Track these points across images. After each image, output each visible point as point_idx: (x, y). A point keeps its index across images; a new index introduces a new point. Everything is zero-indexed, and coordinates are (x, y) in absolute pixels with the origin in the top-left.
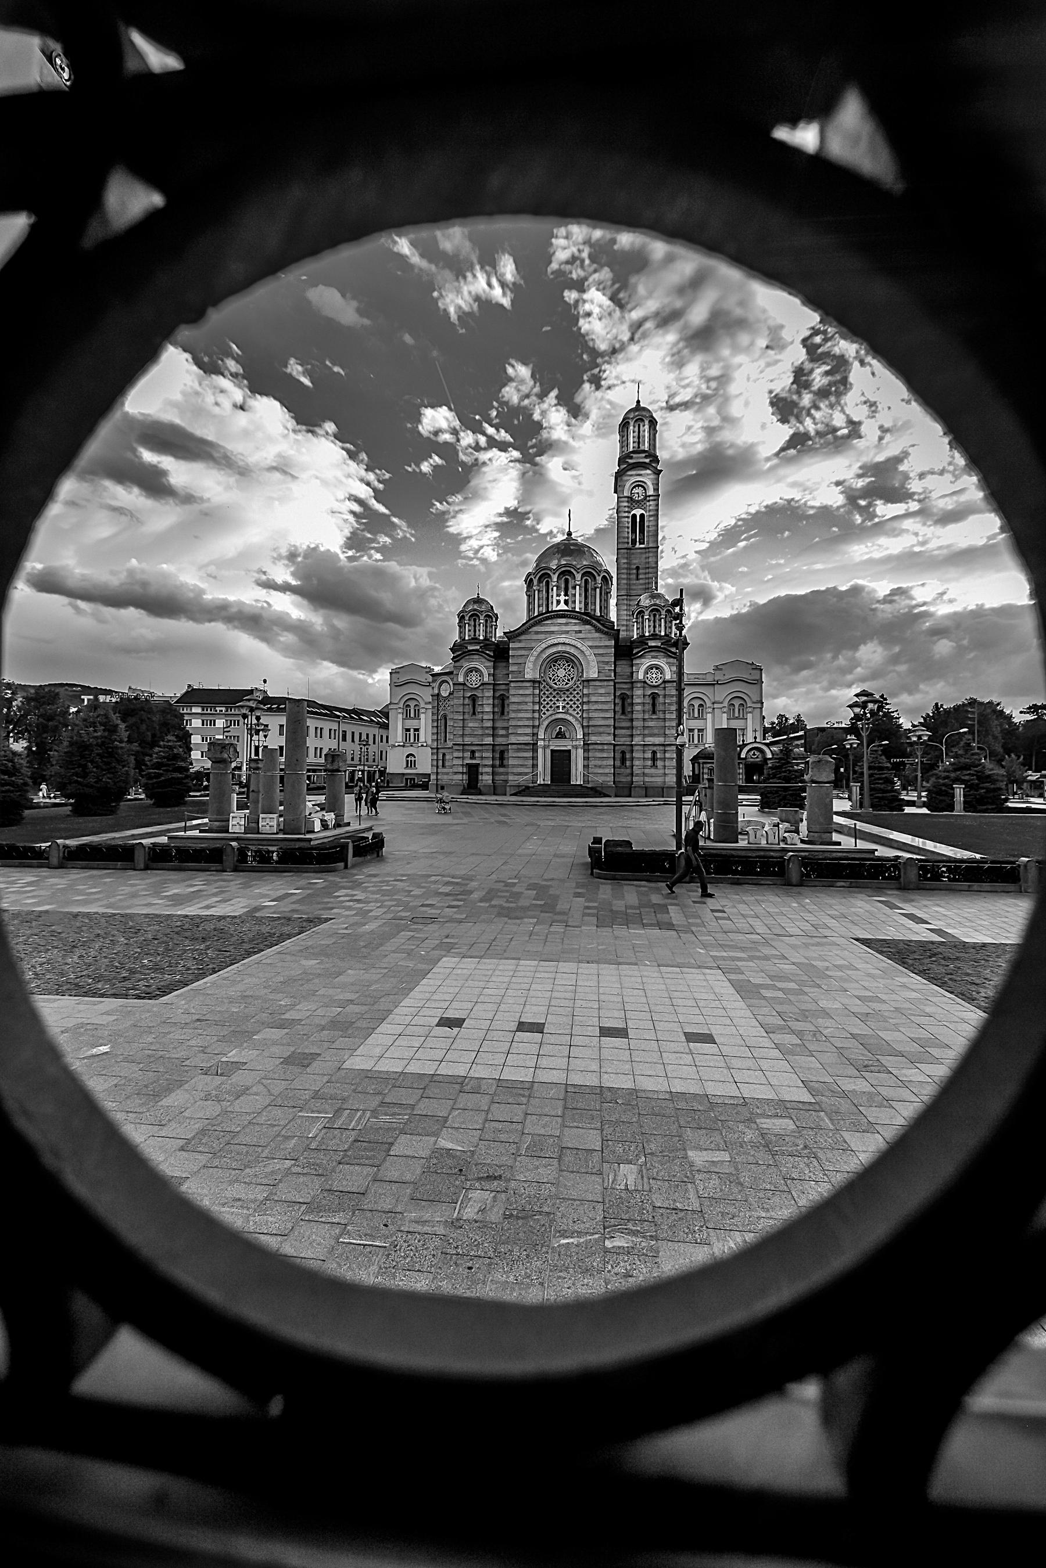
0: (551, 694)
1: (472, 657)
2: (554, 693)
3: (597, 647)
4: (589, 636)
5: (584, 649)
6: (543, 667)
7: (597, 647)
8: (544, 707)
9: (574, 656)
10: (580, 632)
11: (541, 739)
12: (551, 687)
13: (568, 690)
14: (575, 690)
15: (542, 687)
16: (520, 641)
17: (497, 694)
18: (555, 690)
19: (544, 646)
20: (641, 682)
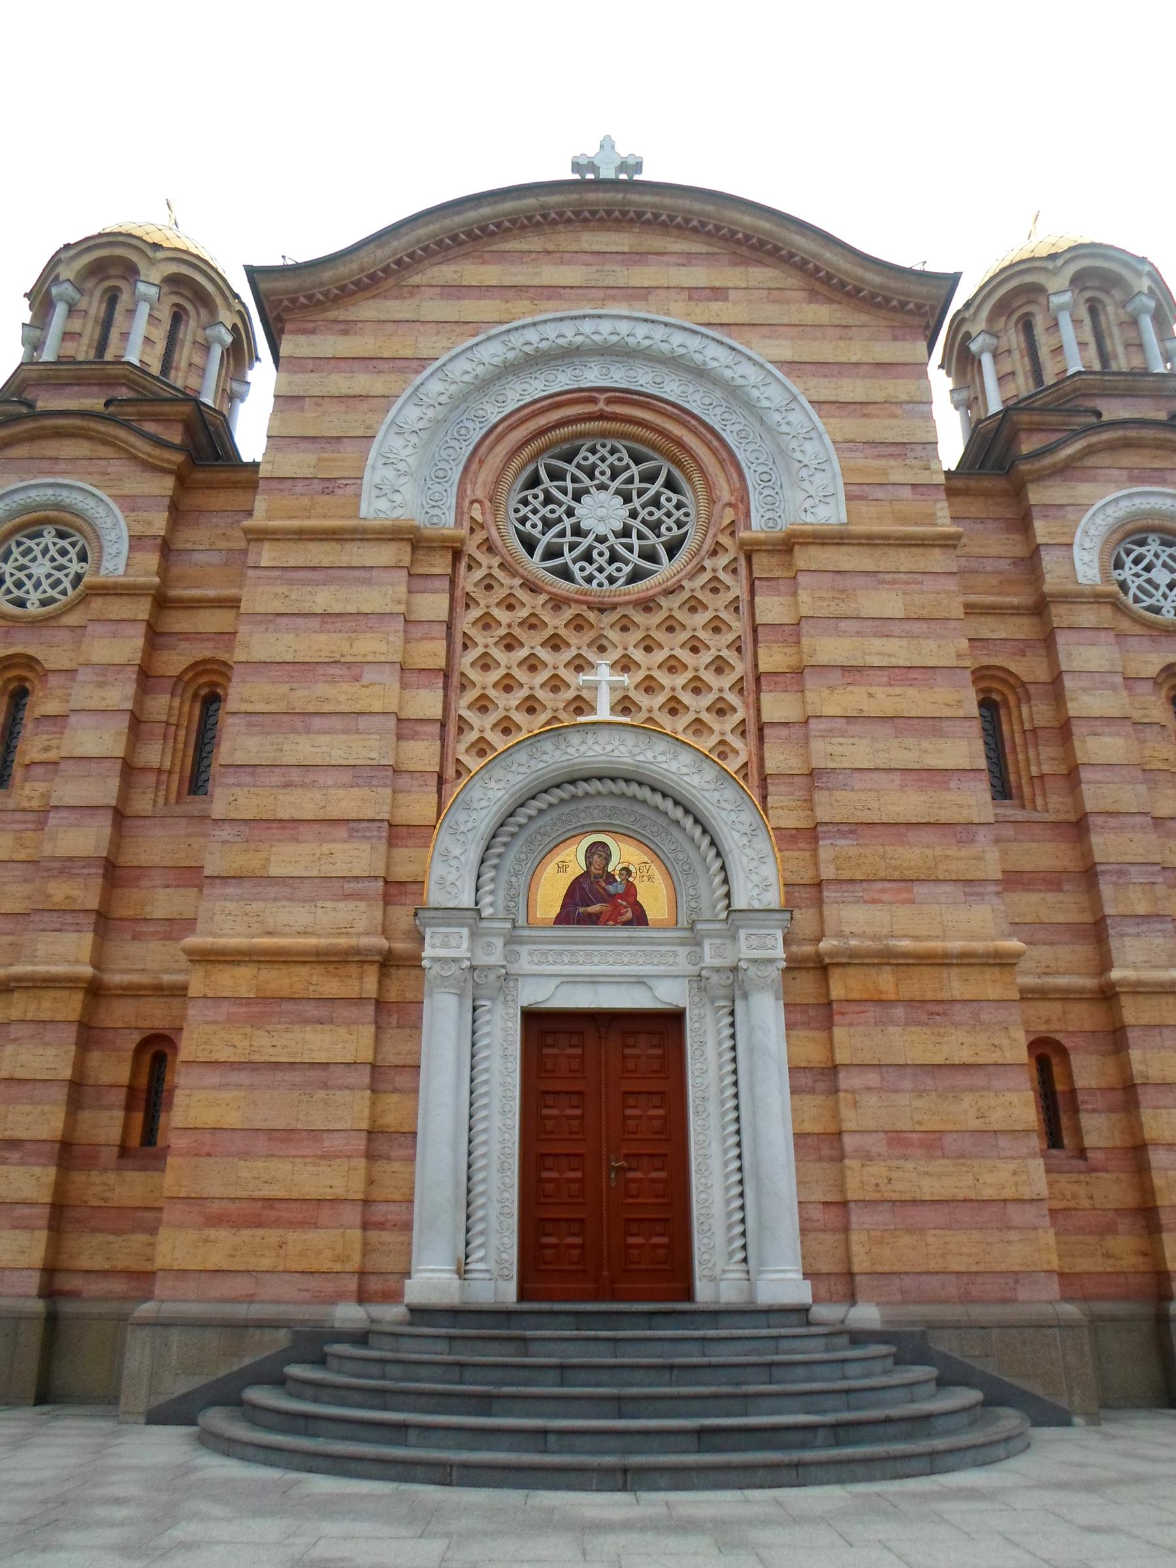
0: (532, 624)
1: (51, 448)
2: (556, 622)
3: (822, 367)
4: (770, 313)
5: (746, 374)
6: (486, 474)
7: (822, 367)
8: (483, 705)
9: (682, 415)
10: (718, 293)
11: (451, 915)
12: (533, 588)
13: (647, 605)
14: (694, 605)
15: (469, 581)
16: (347, 328)
17: (175, 661)
18: (558, 603)
19: (493, 353)
20: (1098, 598)
